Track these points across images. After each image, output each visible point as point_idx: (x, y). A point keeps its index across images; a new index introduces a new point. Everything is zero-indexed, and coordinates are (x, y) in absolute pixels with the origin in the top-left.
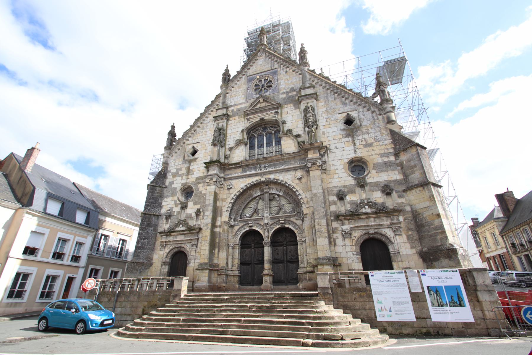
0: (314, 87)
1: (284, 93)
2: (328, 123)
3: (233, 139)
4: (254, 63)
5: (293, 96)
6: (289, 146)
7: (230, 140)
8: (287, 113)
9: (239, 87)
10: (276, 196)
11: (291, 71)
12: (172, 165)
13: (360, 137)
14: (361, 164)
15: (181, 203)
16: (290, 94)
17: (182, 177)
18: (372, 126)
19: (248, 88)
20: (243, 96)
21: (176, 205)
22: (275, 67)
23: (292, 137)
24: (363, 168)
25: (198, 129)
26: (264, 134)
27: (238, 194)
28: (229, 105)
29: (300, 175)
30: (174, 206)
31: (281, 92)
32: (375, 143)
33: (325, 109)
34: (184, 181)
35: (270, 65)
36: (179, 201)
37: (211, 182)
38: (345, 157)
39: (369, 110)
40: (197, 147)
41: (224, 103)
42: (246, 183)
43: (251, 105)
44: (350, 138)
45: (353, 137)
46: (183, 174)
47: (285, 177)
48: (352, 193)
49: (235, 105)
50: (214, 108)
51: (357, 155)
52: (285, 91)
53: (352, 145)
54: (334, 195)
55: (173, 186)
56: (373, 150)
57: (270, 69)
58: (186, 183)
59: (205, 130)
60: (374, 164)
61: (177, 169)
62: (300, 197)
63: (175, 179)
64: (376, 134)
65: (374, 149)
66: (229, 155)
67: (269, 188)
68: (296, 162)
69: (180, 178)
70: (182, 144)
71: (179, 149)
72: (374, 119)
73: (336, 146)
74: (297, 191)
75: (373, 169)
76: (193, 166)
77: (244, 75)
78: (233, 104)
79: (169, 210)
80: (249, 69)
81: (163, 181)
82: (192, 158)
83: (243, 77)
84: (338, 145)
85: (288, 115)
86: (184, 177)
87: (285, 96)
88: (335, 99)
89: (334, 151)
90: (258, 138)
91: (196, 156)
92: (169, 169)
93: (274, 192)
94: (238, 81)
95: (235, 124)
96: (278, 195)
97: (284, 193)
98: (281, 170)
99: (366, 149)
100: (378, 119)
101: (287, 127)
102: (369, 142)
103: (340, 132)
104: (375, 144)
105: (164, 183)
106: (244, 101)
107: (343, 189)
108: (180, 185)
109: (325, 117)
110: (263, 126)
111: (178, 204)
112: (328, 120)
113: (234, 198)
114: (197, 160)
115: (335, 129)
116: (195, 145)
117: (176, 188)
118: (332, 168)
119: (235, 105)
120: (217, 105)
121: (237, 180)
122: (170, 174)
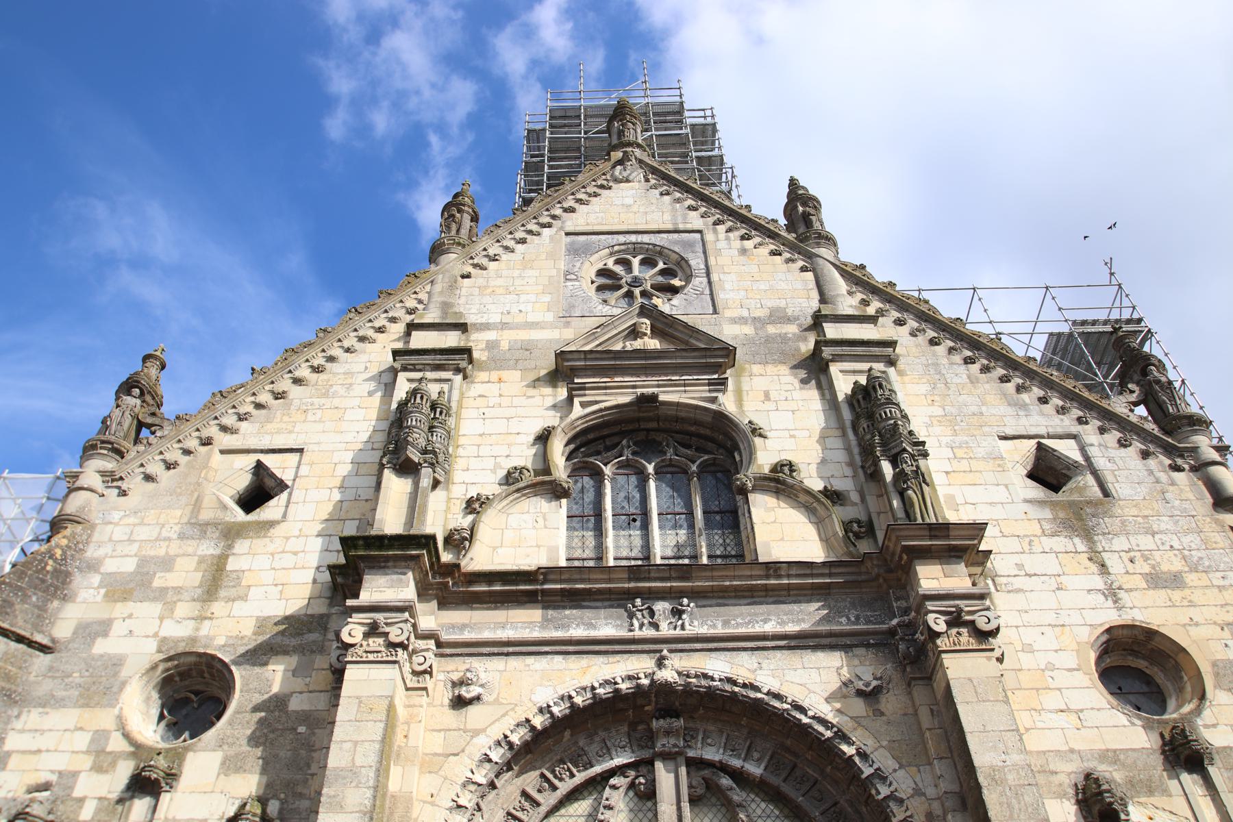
0: (872, 320)
1: (742, 320)
2: (964, 465)
3: (490, 463)
4: (596, 195)
5: (784, 338)
6: (785, 534)
7: (474, 463)
8: (767, 396)
9: (526, 264)
10: (726, 781)
11: (764, 251)
12: (119, 533)
13: (1120, 543)
14: (1141, 664)
15: (138, 749)
16: (771, 330)
17: (170, 608)
18: (1159, 506)
19: (568, 275)
20: (547, 298)
21: (102, 761)
22: (689, 227)
23: (803, 498)
24: (1148, 680)
25: (295, 392)
26: (650, 468)
27: (515, 739)
28: (470, 319)
29: (868, 677)
30: (88, 762)
31: (728, 314)
32: (1194, 576)
33: (940, 412)
34: (181, 629)
35: (667, 217)
36: (127, 736)
37: (376, 643)
38: (1076, 618)
39: (1123, 444)
40: (279, 466)
41: (446, 306)
42: (568, 687)
43: (592, 335)
44: (1077, 540)
45: (1088, 535)
46: (178, 590)
47: (790, 675)
48: (1151, 792)
49: (504, 326)
50: (393, 320)
51: (1127, 618)
52: (745, 313)
53: (1094, 568)
54: (1062, 796)
55: (102, 647)
56: (1192, 604)
57: (670, 227)
58: (193, 640)
59: (336, 402)
60: (1214, 664)
61: (143, 561)
62: (884, 791)
63: (120, 609)
64: (1186, 540)
65: (1195, 598)
66: (472, 529)
67: (689, 735)
68: (840, 613)
69: (156, 608)
70: (192, 443)
71: (169, 466)
72: (1158, 481)
73: (1020, 566)
74: (863, 755)
75: (1218, 685)
76: (248, 558)
77: (549, 226)
78: (495, 318)
79: (46, 787)
80: (571, 210)
81: (42, 608)
82: (239, 515)
83: (546, 231)
84: (1033, 563)
85: (770, 406)
86: (184, 609)
87: (748, 330)
88: (973, 381)
89: (1018, 583)
90: (613, 480)
91: (271, 510)
92: (91, 552)
93: (712, 754)
94: (523, 241)
95: (505, 401)
96: (739, 777)
97: (773, 765)
98: (764, 637)
99: (1161, 595)
100: (1173, 484)
101: (765, 457)
102: (1165, 567)
103: (1026, 507)
104: (1191, 578)
105: (42, 616)
106: (550, 317)
107: (1103, 770)
108: (152, 646)
109: (944, 440)
110: (641, 436)
111: (116, 757)
112: (960, 453)
113: (496, 755)
114: (276, 531)
115: (1000, 494)
116: (269, 461)
117: (115, 663)
118: (1026, 660)
119: (504, 326)
120: (411, 312)
121: (514, 662)
122: (96, 579)
